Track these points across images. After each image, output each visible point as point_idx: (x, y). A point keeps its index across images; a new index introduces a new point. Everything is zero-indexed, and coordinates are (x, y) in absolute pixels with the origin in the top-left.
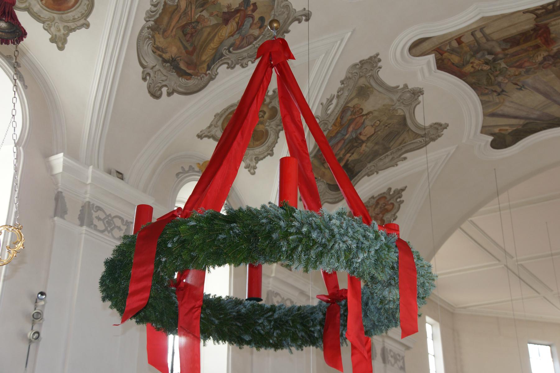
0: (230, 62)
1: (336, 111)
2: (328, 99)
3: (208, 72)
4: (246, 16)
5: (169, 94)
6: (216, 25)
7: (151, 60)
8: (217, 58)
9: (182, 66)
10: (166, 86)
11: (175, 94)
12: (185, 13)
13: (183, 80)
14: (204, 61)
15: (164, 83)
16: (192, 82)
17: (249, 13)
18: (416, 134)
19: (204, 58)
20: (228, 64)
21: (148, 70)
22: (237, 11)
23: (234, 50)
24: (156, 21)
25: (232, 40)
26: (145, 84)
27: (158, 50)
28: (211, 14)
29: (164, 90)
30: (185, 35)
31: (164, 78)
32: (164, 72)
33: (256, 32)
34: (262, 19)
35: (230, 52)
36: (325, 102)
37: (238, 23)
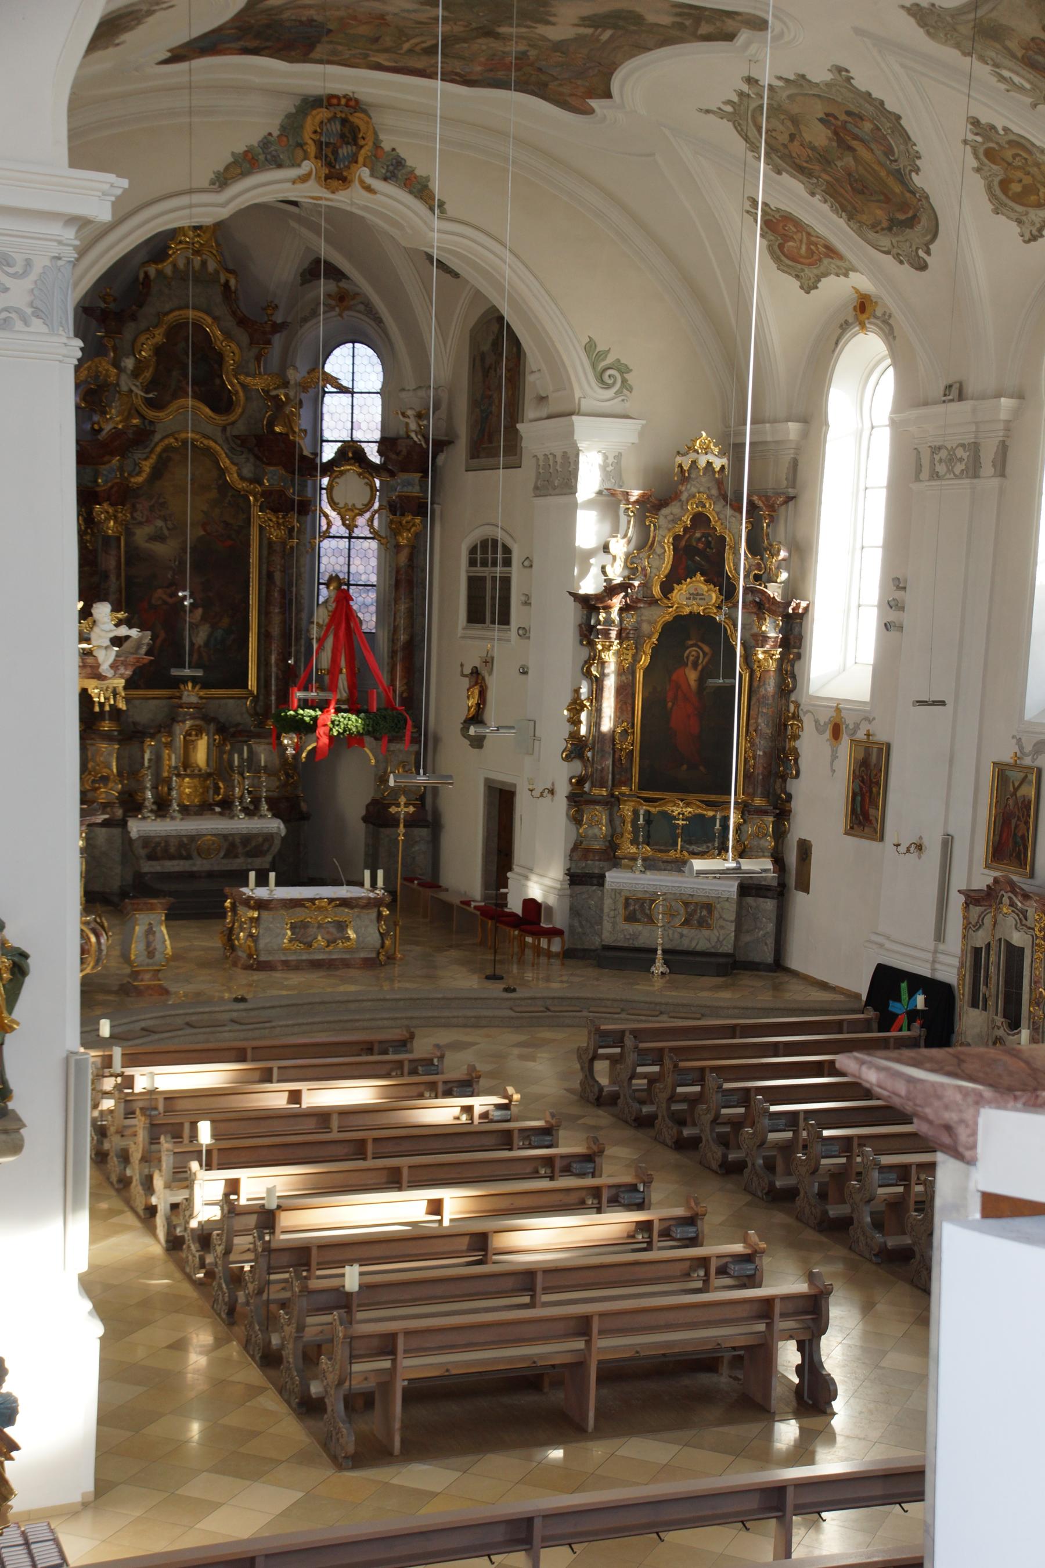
0: (909, 168)
1: (1028, 76)
2: (999, 81)
3: (918, 195)
4: (844, 128)
5: (928, 252)
6: (855, 158)
7: (885, 241)
8: (901, 177)
9: (901, 217)
10: (917, 249)
11: (931, 247)
12: (837, 180)
13: (918, 228)
14: (902, 192)
15: (914, 248)
16: (924, 221)
17: (839, 123)
18: (622, 382)
19: (897, 191)
20: (911, 171)
21: (895, 251)
22: (836, 133)
23: (893, 156)
24: (843, 210)
25: (878, 153)
26: (906, 266)
27: (874, 226)
28: (839, 158)
29: (921, 253)
30: (863, 193)
31: (908, 244)
32: (900, 238)
33: (868, 126)
34: (849, 113)
35: (896, 161)
36: (1003, 86)
37: (854, 139)
